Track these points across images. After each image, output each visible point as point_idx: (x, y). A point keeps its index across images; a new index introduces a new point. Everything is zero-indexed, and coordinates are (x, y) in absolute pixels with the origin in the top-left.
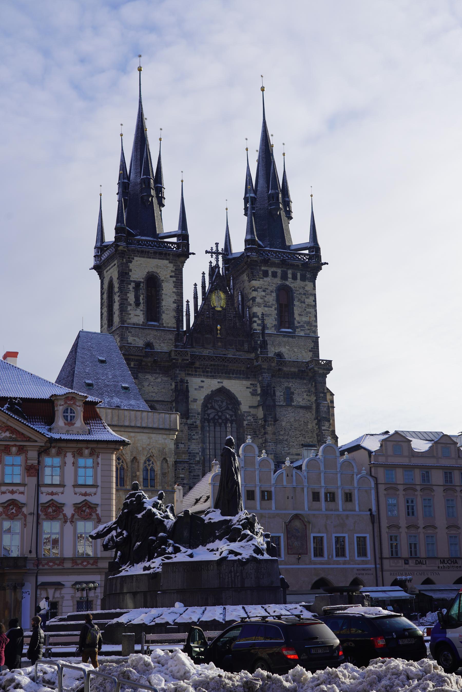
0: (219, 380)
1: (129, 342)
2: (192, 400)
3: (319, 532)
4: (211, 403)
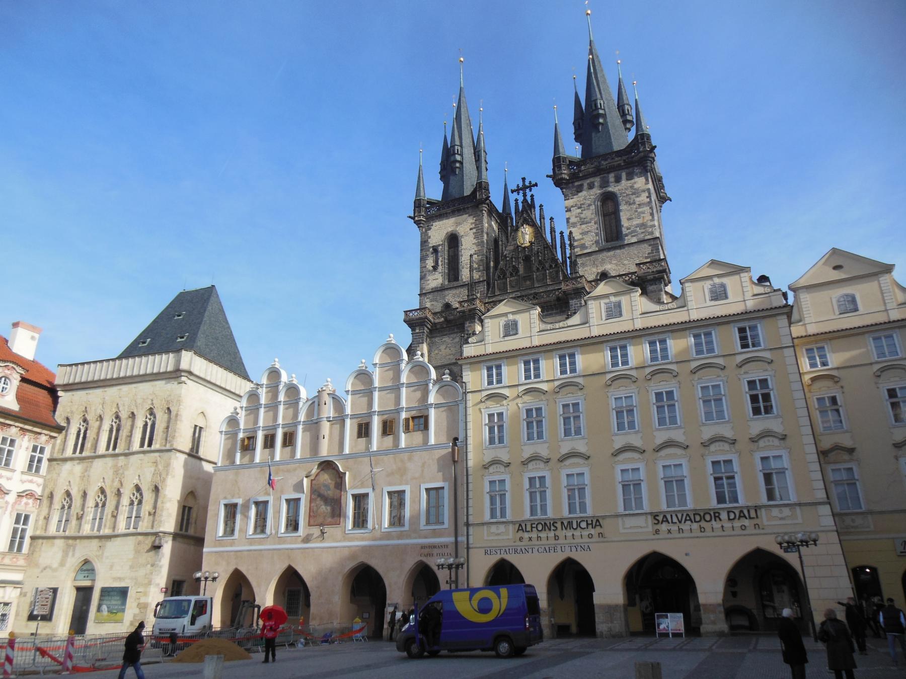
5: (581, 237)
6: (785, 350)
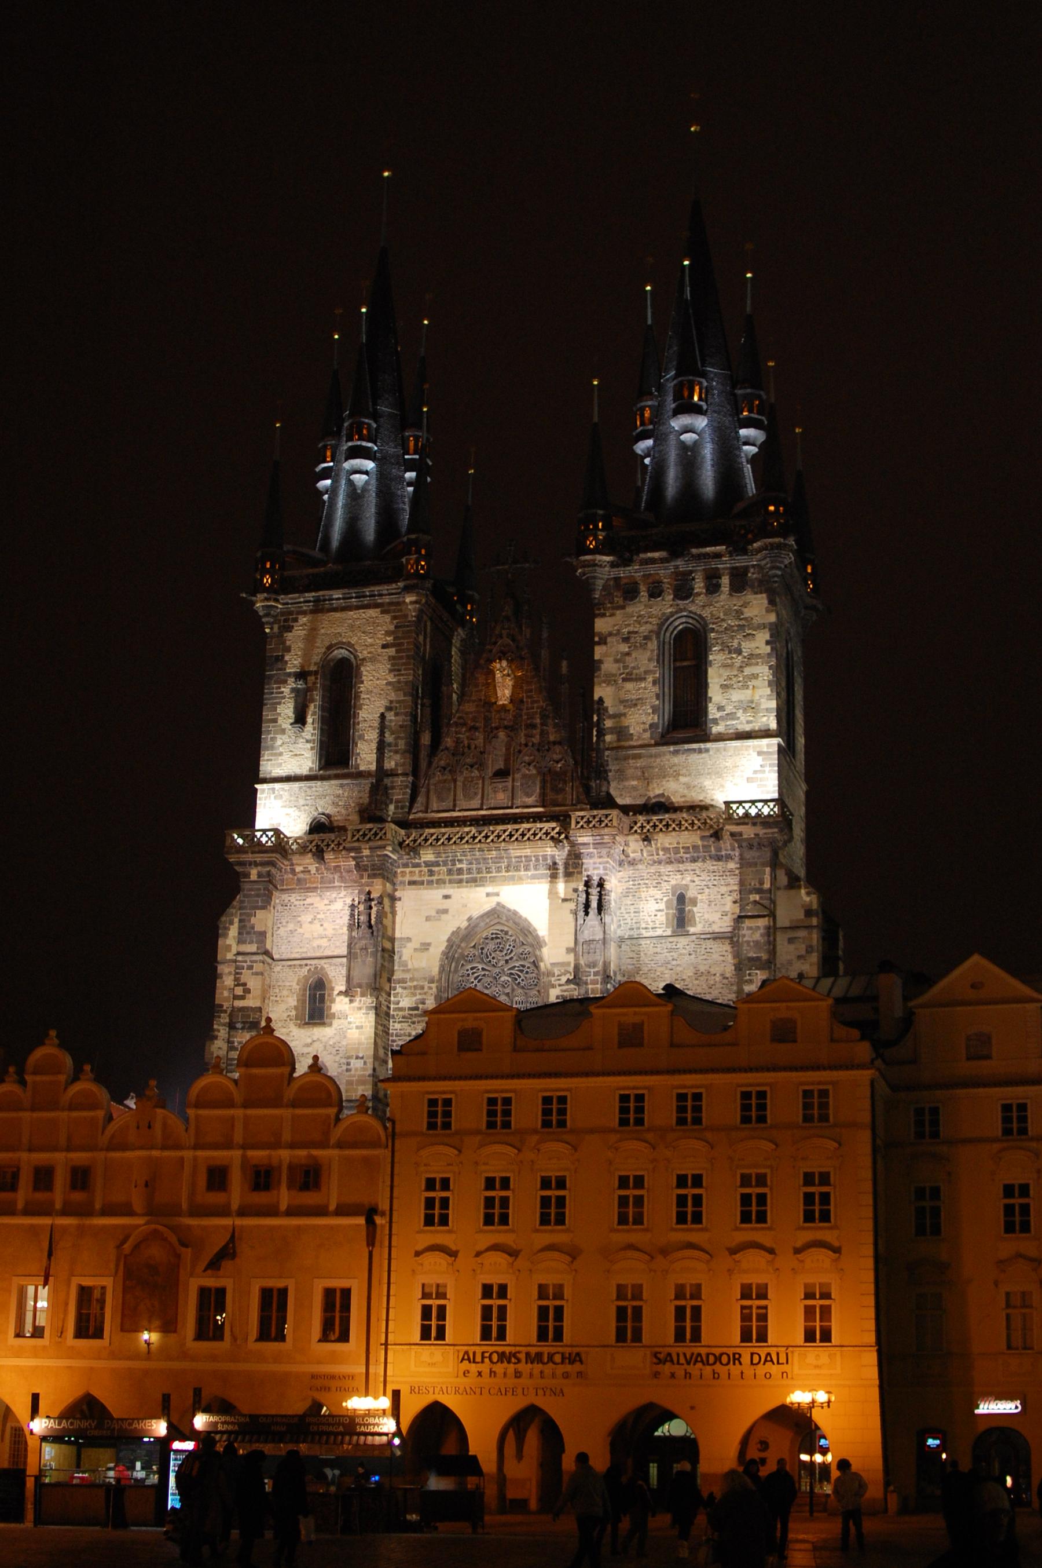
0: (490, 889)
2: (418, 946)
5: (622, 709)
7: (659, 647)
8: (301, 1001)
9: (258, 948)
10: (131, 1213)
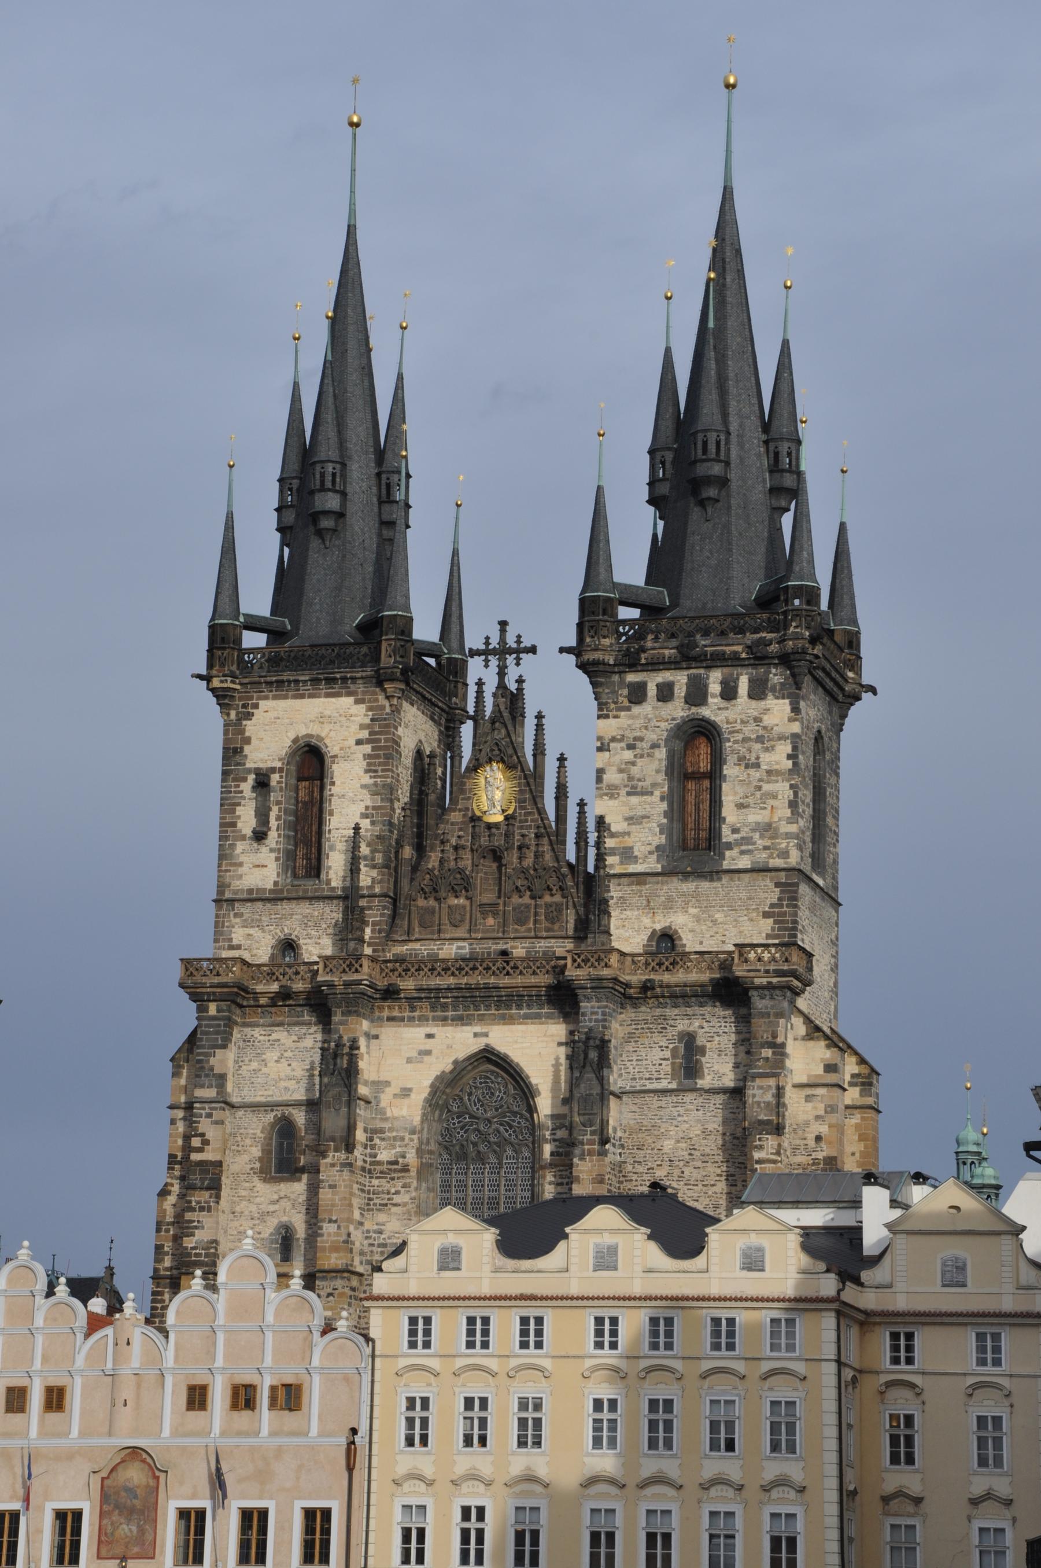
0: (478, 1029)
1: (235, 942)
2: (398, 1091)
3: (194, 1497)
4: (461, 1099)
6: (823, 1363)
7: (667, 757)
8: (266, 1152)
9: (218, 1093)
10: (110, 1434)
